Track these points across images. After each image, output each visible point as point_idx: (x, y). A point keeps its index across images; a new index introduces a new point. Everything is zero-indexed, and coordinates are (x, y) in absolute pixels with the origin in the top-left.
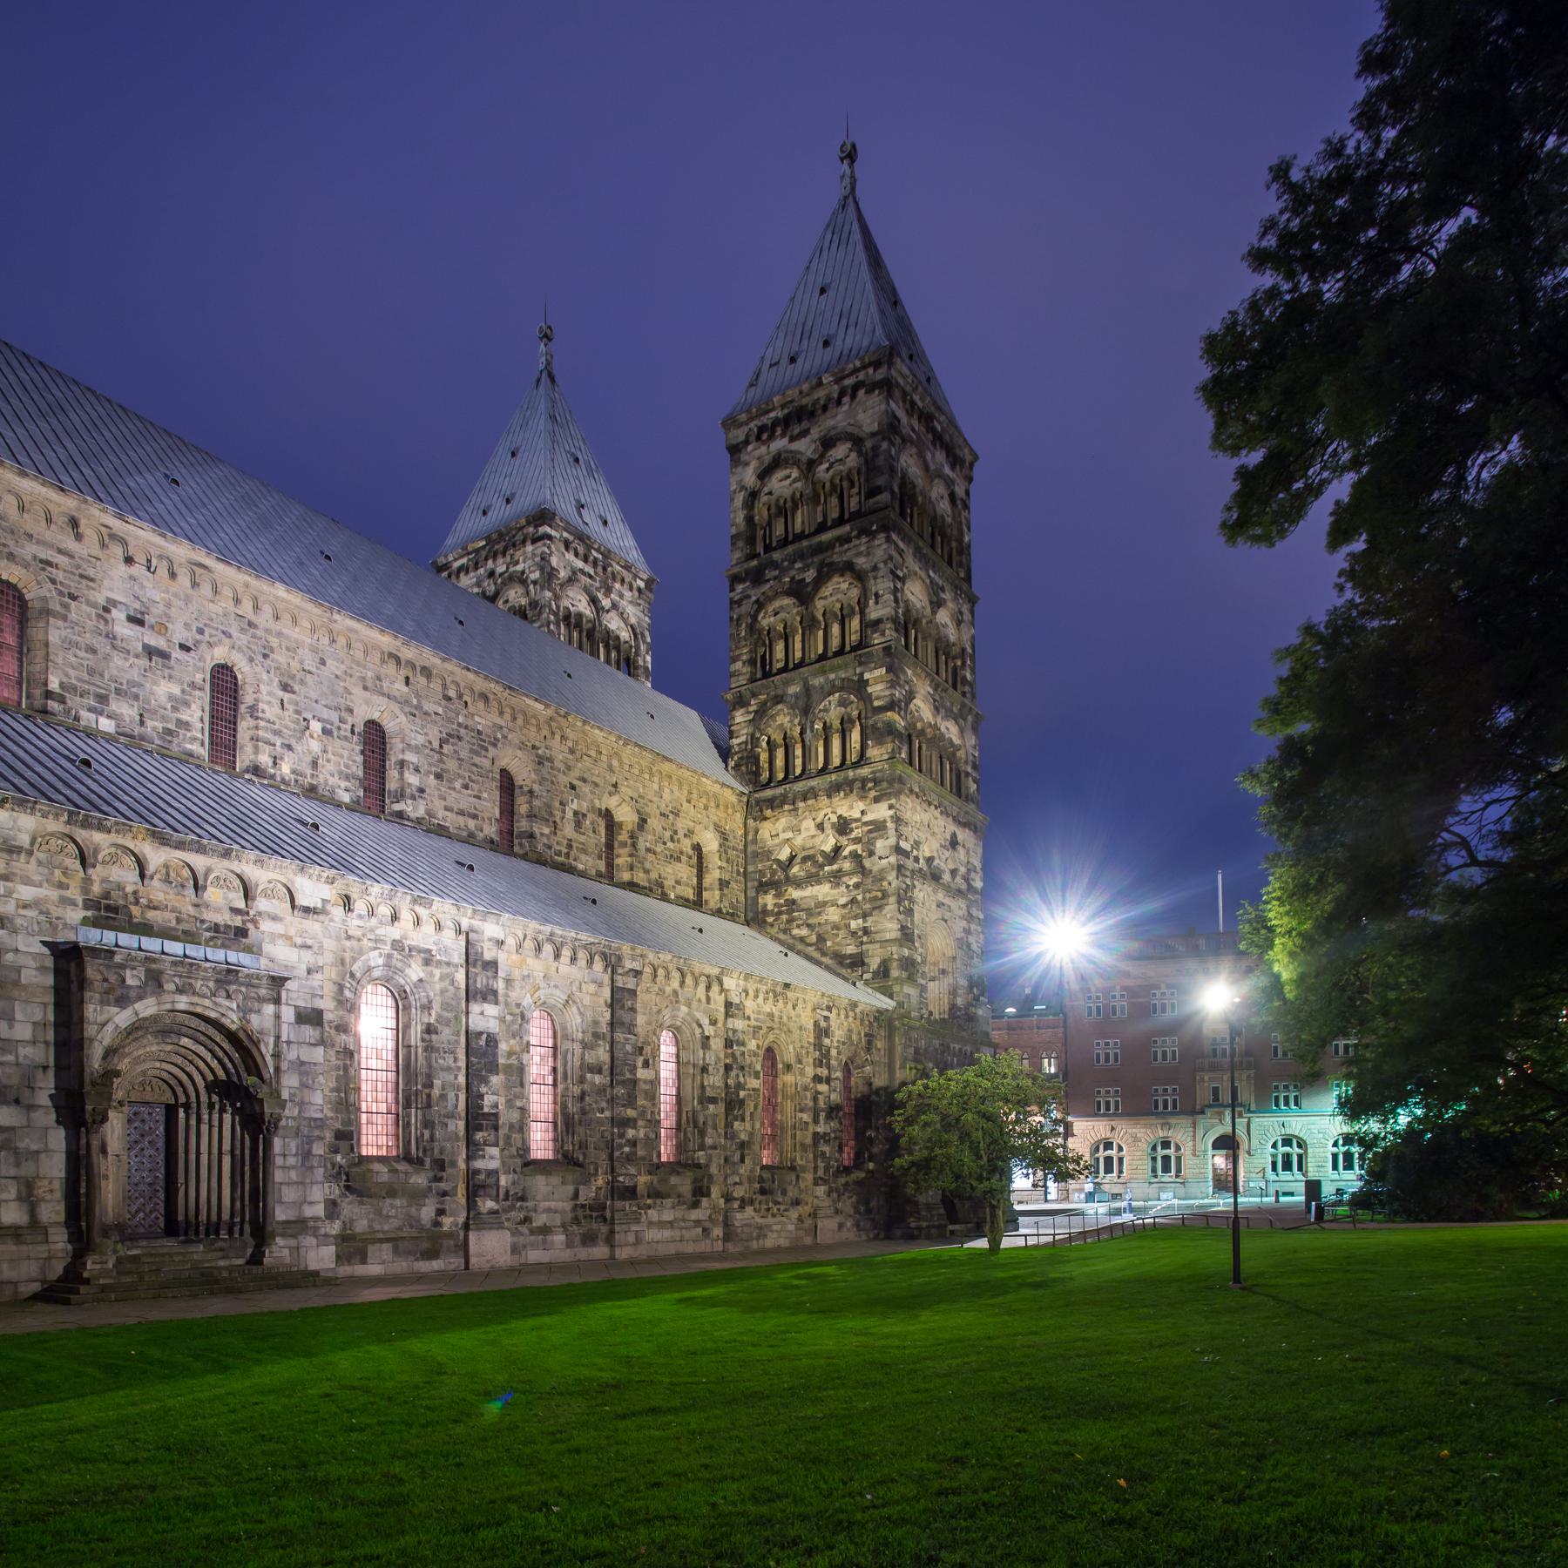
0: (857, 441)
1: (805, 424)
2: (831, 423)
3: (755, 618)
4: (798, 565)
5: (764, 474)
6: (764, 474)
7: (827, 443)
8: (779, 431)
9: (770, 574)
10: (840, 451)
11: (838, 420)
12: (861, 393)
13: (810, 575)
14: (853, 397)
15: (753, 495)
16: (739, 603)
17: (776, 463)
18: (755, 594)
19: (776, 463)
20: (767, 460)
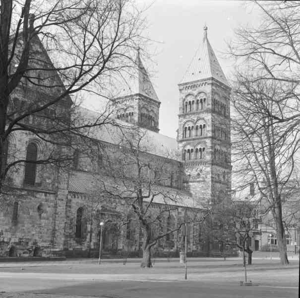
0: (206, 94)
1: (195, 88)
2: (200, 89)
3: (184, 125)
4: (193, 116)
5: (187, 96)
6: (187, 96)
7: (200, 93)
8: (190, 88)
9: (187, 117)
10: (202, 95)
11: (201, 89)
12: (206, 84)
13: (196, 119)
14: (205, 85)
15: (184, 100)
16: (181, 122)
17: (189, 95)
18: (185, 120)
19: (189, 95)
20: (188, 93)
